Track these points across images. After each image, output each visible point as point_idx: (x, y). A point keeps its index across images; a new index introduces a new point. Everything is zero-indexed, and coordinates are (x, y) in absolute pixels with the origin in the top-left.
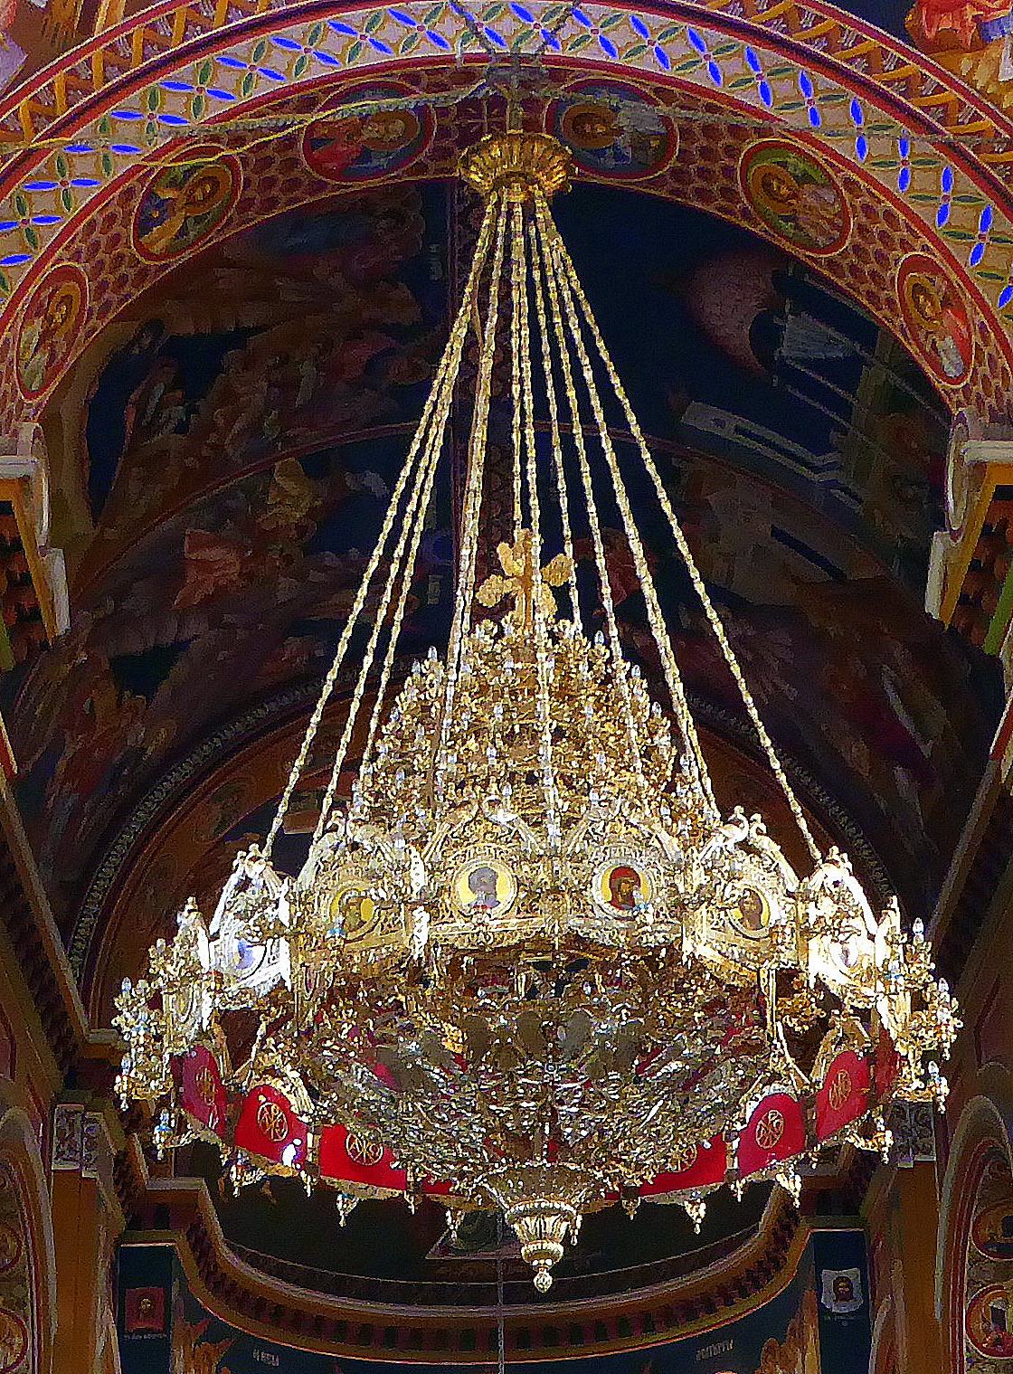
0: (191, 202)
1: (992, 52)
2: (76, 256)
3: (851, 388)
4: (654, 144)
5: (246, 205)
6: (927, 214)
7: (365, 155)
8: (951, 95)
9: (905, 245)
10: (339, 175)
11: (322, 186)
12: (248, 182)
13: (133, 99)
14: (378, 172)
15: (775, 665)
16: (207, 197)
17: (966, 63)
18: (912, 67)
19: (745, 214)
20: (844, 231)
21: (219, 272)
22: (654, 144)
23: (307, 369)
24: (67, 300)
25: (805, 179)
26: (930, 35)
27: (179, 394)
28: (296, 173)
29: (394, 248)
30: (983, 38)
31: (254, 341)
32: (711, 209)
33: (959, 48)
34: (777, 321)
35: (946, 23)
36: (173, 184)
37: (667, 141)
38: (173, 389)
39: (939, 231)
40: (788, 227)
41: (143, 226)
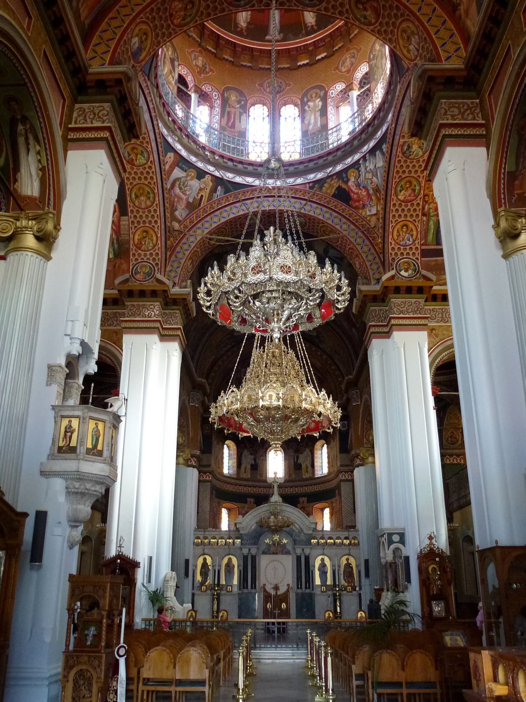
2: (198, 248)
6: (352, 240)
8: (358, 217)
9: (349, 245)
13: (208, 218)
17: (360, 211)
18: (351, 212)
24: (196, 255)
26: (354, 206)
30: (364, 206)
33: (359, 208)
35: (357, 204)
39: (355, 243)
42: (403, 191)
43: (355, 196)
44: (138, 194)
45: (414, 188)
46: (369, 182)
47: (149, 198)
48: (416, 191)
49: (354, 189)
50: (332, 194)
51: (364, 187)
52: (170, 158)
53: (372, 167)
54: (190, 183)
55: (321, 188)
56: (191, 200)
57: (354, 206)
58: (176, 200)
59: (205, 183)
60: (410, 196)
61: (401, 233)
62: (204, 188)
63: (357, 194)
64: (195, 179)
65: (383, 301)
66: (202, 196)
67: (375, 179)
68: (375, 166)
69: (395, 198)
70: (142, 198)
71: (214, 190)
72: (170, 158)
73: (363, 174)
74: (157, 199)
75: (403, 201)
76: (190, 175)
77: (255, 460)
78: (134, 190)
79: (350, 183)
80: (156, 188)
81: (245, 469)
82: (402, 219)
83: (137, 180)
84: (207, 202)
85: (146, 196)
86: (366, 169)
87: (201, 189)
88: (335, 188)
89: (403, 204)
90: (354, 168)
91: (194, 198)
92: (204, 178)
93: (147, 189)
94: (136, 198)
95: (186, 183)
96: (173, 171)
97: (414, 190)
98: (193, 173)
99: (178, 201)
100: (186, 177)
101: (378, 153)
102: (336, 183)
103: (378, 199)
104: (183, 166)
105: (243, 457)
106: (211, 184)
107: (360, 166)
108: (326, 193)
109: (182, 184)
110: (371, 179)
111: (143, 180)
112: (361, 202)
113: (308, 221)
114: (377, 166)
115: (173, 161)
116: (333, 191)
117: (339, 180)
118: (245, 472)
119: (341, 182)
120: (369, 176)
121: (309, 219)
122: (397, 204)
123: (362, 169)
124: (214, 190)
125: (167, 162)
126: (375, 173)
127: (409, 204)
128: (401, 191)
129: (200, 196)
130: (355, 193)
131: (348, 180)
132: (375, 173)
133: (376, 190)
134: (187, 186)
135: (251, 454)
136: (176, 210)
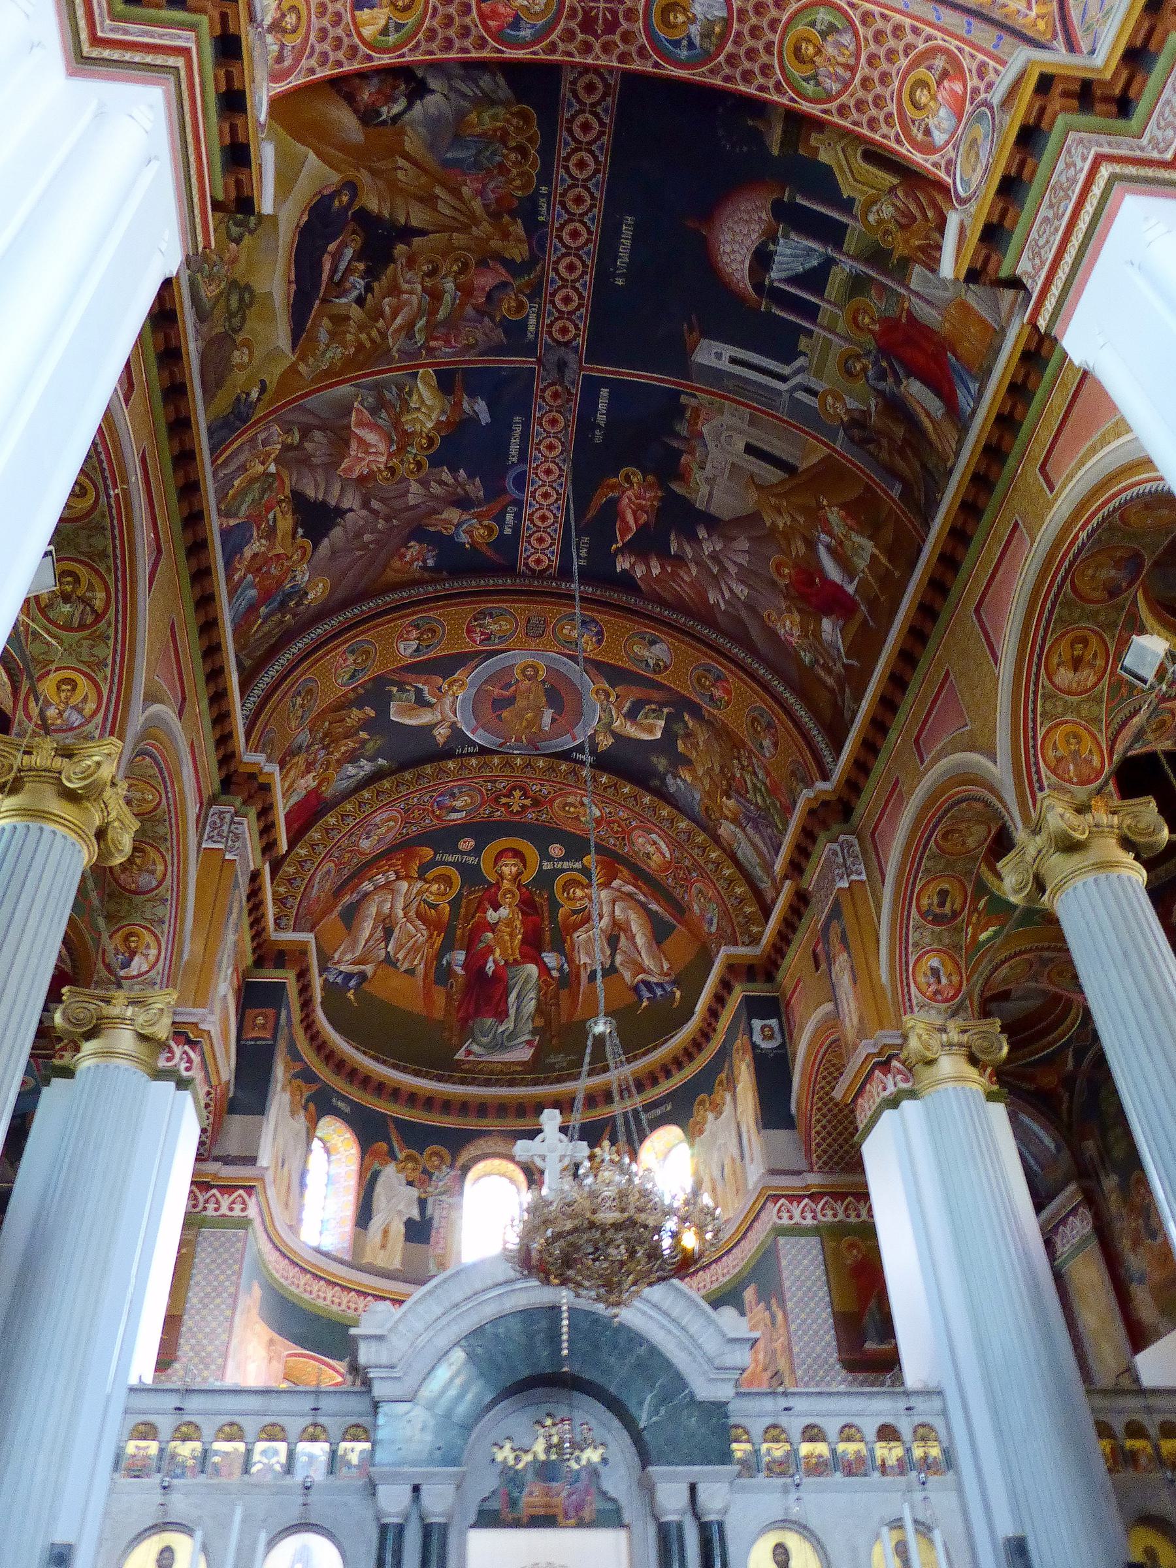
3: (819, 291)
4: (717, 29)
7: (516, 23)
15: (733, 570)
19: (778, 87)
20: (852, 69)
21: (401, 162)
22: (717, 29)
23: (450, 286)
25: (832, 29)
27: (361, 266)
31: (416, 241)
32: (752, 91)
34: (771, 247)
38: (358, 260)
40: (809, 88)
65: (1123, 106)
77: (422, 1203)
81: (386, 1232)
105: (379, 1189)
118: (383, 1246)
135: (410, 1183)
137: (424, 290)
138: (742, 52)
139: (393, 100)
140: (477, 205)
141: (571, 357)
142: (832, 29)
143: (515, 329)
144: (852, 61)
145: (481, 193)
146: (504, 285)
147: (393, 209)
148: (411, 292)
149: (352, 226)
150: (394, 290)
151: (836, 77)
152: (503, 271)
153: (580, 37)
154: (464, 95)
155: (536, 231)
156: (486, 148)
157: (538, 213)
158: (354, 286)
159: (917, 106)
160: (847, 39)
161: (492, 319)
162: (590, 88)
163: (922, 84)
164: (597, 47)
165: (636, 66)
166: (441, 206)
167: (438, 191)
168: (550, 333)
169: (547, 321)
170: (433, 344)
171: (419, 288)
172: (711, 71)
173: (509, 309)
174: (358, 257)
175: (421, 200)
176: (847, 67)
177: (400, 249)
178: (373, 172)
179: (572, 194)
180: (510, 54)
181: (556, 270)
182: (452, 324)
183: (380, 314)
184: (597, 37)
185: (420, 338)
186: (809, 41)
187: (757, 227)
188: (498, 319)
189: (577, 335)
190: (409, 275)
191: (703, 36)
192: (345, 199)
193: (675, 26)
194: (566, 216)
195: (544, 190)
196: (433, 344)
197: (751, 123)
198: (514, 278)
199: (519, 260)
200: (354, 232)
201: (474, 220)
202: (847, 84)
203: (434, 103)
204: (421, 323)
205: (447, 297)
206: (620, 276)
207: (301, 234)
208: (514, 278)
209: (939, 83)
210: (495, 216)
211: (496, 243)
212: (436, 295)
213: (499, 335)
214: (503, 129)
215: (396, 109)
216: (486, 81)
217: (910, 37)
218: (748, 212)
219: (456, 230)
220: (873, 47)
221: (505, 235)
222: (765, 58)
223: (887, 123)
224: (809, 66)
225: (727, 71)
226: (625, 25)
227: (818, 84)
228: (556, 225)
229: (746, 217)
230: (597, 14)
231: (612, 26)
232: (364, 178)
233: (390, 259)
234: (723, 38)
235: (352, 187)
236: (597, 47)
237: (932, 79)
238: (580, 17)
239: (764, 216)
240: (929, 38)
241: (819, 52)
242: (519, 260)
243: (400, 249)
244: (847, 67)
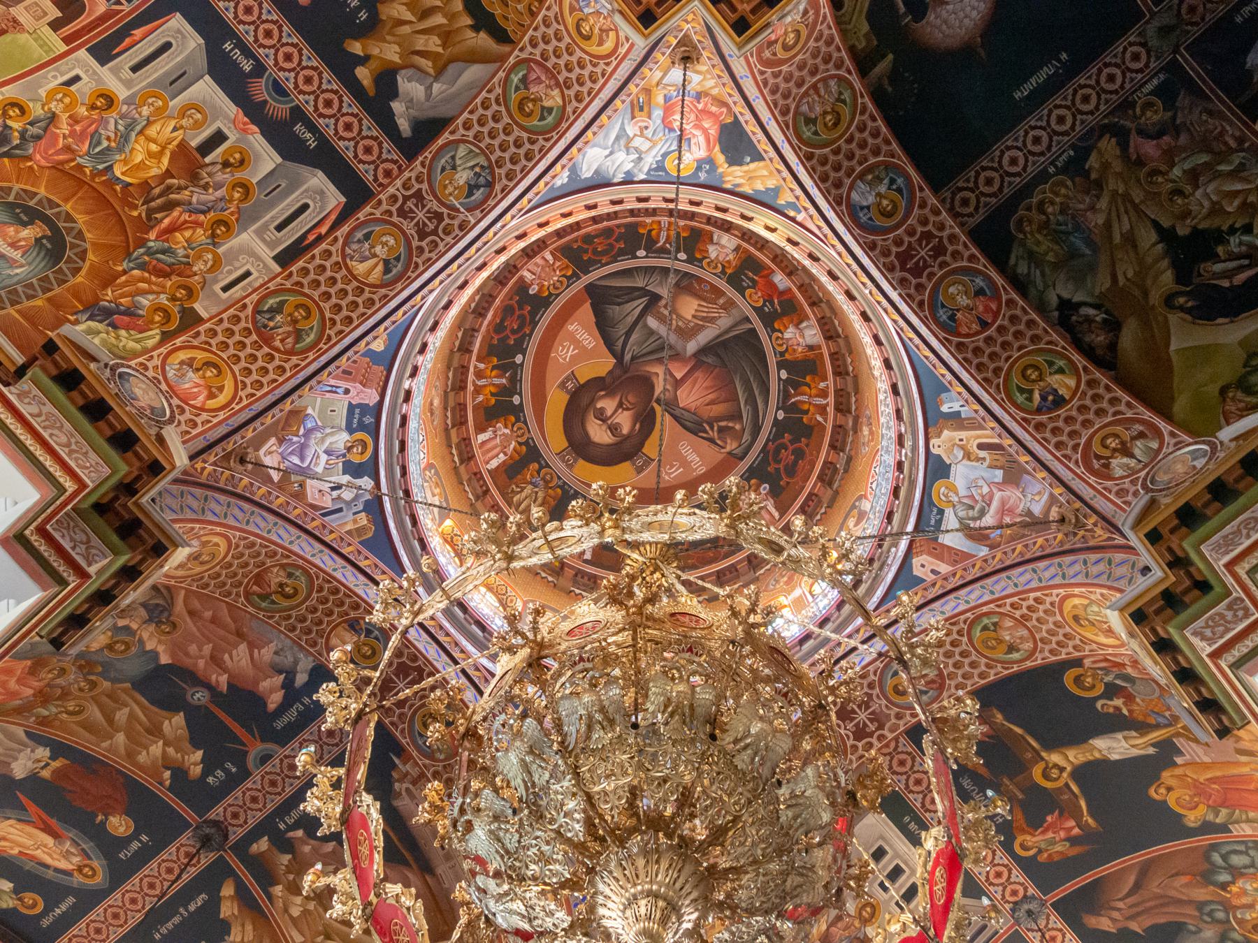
0: (1041, 378)
1: (699, 89)
4: (870, 177)
5: (1035, 339)
7: (980, 292)
10: (999, 299)
11: (1010, 302)
12: (1020, 348)
14: (988, 278)
16: (1036, 367)
17: (715, 92)
20: (814, 87)
22: (870, 177)
23: (1177, 172)
27: (1220, 250)
28: (1006, 323)
29: (1063, 191)
30: (699, 96)
31: (1166, 223)
35: (714, 109)
36: (1030, 399)
37: (861, 176)
40: (847, 95)
41: (1060, 402)
42: (547, 104)
43: (706, 126)
44: (1005, 648)
45: (522, 86)
46: (649, 133)
47: (995, 624)
48: (520, 75)
49: (701, 139)
50: (762, 164)
51: (672, 130)
52: (923, 566)
53: (621, 156)
54: (962, 492)
55: (776, 191)
56: (999, 475)
57: (724, 110)
58: (1007, 520)
59: (950, 451)
60: (538, 81)
61: (596, 31)
62: (962, 447)
63: (697, 127)
64: (951, 479)
66: (981, 447)
67: (631, 130)
68: (611, 153)
69: (569, 109)
70: (1007, 638)
71: (955, 420)
72: (923, 566)
73: (654, 152)
74: (985, 609)
75: (558, 84)
76: (946, 496)
78: (1001, 656)
79: (702, 153)
80: (962, 617)
82: (579, 53)
83: (974, 658)
84: (983, 428)
85: (995, 631)
86: (640, 159)
87: (968, 456)
88: (745, 168)
89: (561, 79)
90: (667, 173)
91: (990, 467)
92: (939, 456)
93: (977, 633)
94: (1018, 650)
95: (965, 501)
96: (949, 547)
97: (524, 80)
98: (940, 489)
99: (1011, 511)
100: (954, 506)
101: (586, 173)
102: (735, 176)
103: (648, 91)
104: (933, 522)
106: (946, 433)
107: (650, 170)
108: (771, 173)
109: (971, 513)
110: (642, 135)
111: (964, 647)
112: (700, 106)
113: (848, 182)
114: (607, 152)
115: (930, 554)
116: (753, 166)
117: (722, 175)
119: (720, 170)
120: (638, 142)
121: (838, 185)
122: (572, 93)
123: (649, 161)
124: (955, 420)
125: (933, 571)
126: (622, 142)
127: (549, 65)
128: (550, 110)
129: (982, 454)
130: (705, 131)
131: (700, 164)
132: (622, 142)
133: (641, 109)
134: (972, 497)
136: (1029, 513)
137: (1197, 187)
138: (867, 151)
139: (1089, 320)
140: (1103, 204)
141: (1151, 30)
142: (809, 121)
143: (1166, 93)
144: (811, 92)
145: (1092, 208)
146: (1141, 132)
147: (1157, 261)
148: (1207, 195)
149: (1196, 280)
150: (1216, 210)
151: (827, 86)
152: (1132, 144)
153: (950, 248)
154: (1043, 275)
155: (1082, 151)
156: (1062, 232)
157: (1070, 159)
158: (1241, 243)
159: (798, 32)
160: (805, 108)
161: (1174, 118)
162: (965, 202)
163: (786, 48)
164: (945, 234)
165: (933, 201)
166: (1126, 227)
167: (1117, 239)
168: (1147, 66)
169: (1140, 76)
170: (1233, 144)
171: (1199, 193)
172: (893, 157)
173: (1156, 112)
174: (1216, 258)
175: (1135, 247)
176: (817, 92)
177: (1182, 231)
178: (1146, 293)
179: (1037, 149)
180: (999, 281)
181: (1097, 108)
182: (1204, 144)
183: (1244, 204)
184: (941, 238)
185: (1237, 159)
186: (825, 125)
187: (944, 12)
188: (1170, 114)
189: (1131, 44)
190: (1194, 208)
191: (881, 180)
192: (1182, 300)
193: (892, 201)
194: (1055, 138)
195: (1052, 170)
196: (1233, 144)
197: (890, 89)
198: (1129, 131)
199: (1114, 140)
200: (1200, 275)
201: (1115, 193)
202: (824, 80)
203: (1064, 289)
204: (1223, 168)
205: (1187, 166)
206: (1059, 61)
207: (1236, 315)
208: (1129, 131)
209: (776, 41)
210: (1099, 185)
211: (1117, 166)
212: (1194, 176)
213: (1183, 100)
214: (1039, 231)
215: (1091, 312)
216: (1022, 269)
217: (771, 81)
218: (941, 31)
219: (1132, 202)
220: (794, 91)
221: (1106, 166)
222: (857, 135)
223: (821, 35)
224: (836, 109)
225: (884, 148)
226: (919, 229)
227: (840, 93)
228: (1066, 138)
229: (944, 27)
230: (930, 250)
231: (927, 236)
232: (1155, 297)
233: (1196, 232)
234: (869, 170)
235: (1169, 301)
236: (945, 234)
237: (778, 47)
238: (940, 259)
239: (933, 16)
240: (762, 73)
241: (825, 113)
242: (1114, 140)
243: (1182, 231)
244: (817, 92)
